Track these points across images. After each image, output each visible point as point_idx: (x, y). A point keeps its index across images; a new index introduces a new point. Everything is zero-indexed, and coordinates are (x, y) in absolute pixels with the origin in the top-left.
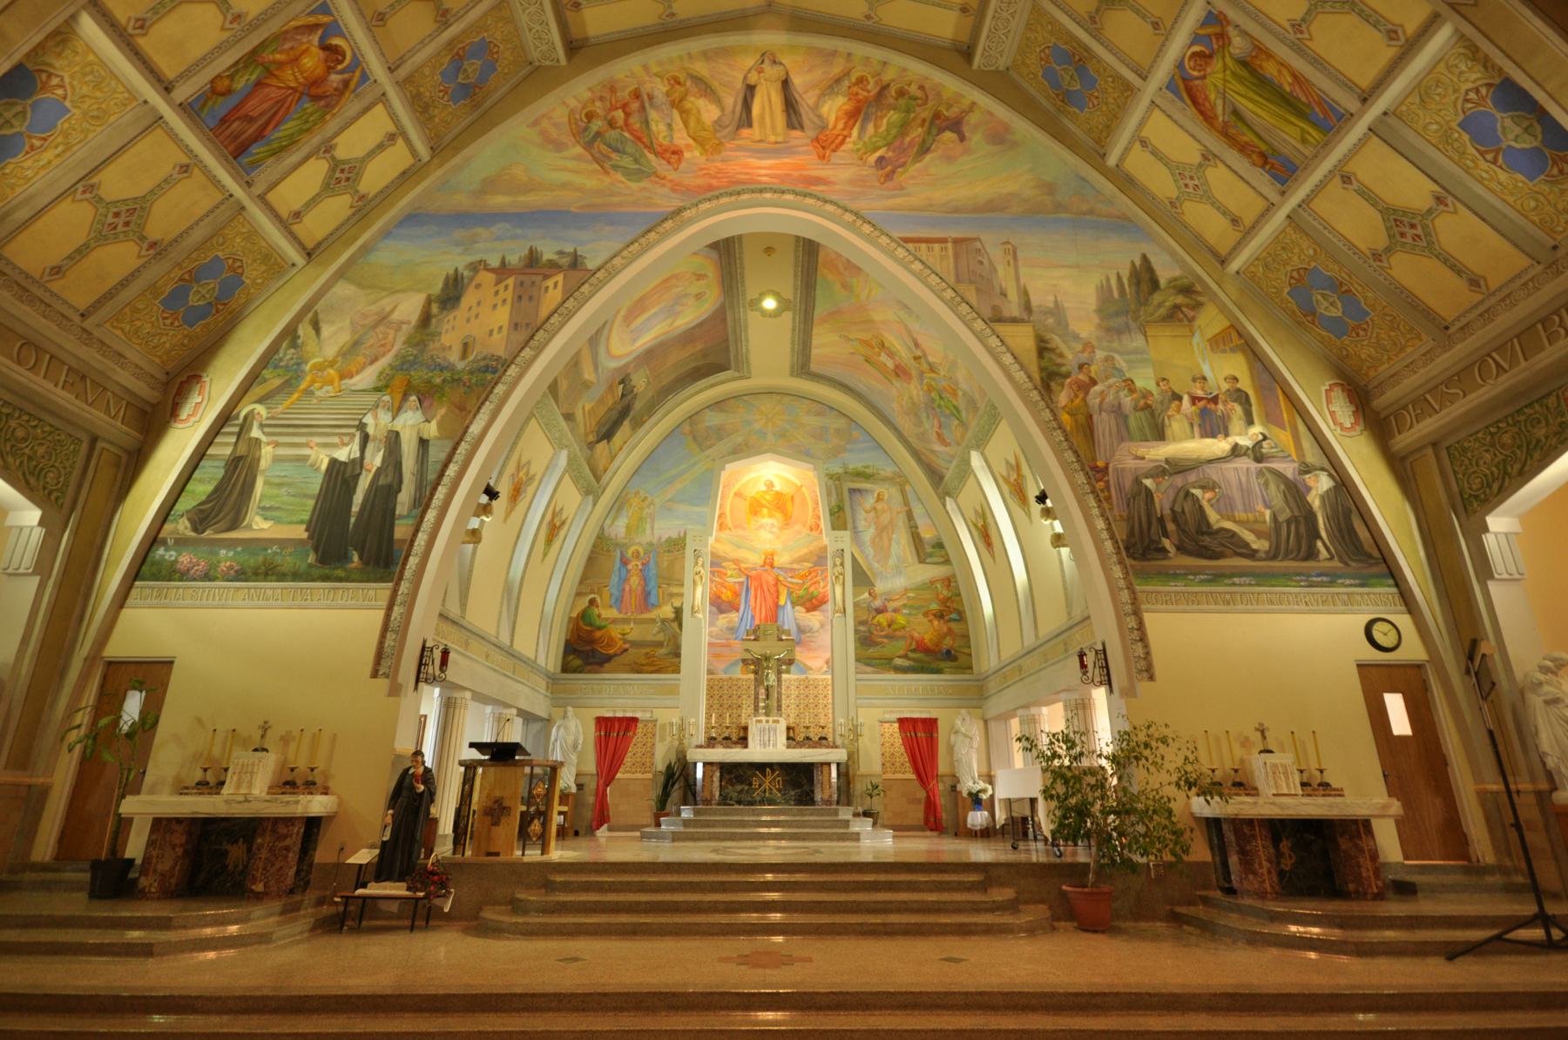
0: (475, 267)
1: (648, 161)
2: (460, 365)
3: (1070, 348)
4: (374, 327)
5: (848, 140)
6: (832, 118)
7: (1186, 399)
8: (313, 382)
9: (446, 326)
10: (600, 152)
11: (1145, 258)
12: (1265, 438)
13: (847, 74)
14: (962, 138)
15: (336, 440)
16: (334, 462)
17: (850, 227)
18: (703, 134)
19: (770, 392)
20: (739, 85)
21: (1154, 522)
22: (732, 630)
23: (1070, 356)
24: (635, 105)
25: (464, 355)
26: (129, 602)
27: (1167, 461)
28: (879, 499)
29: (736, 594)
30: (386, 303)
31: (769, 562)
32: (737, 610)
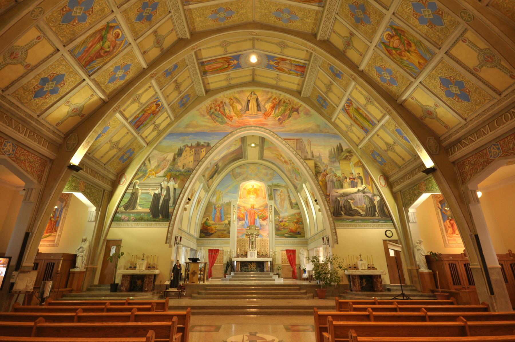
0: (185, 146)
2: (183, 170)
3: (322, 166)
4: (163, 161)
6: (268, 108)
7: (348, 178)
8: (149, 175)
9: (179, 161)
11: (340, 144)
12: (365, 188)
13: (271, 97)
14: (298, 114)
15: (155, 188)
16: (155, 194)
17: (272, 135)
18: (238, 112)
19: (253, 163)
20: (246, 100)
21: (340, 208)
22: (243, 225)
23: (322, 168)
25: (183, 168)
26: (111, 226)
27: (343, 193)
28: (281, 192)
29: (244, 216)
30: (165, 155)
31: (253, 207)
32: (244, 220)
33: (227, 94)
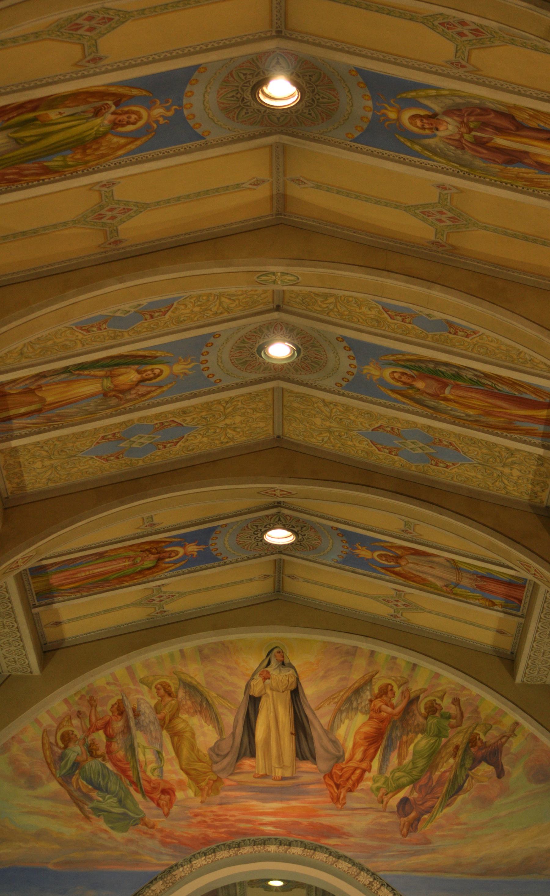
1: (135, 803)
5: (367, 775)
6: (350, 745)
10: (79, 789)
13: (368, 682)
14: (500, 773)
18: (198, 766)
20: (241, 697)
24: (118, 725)
33: (147, 665)
